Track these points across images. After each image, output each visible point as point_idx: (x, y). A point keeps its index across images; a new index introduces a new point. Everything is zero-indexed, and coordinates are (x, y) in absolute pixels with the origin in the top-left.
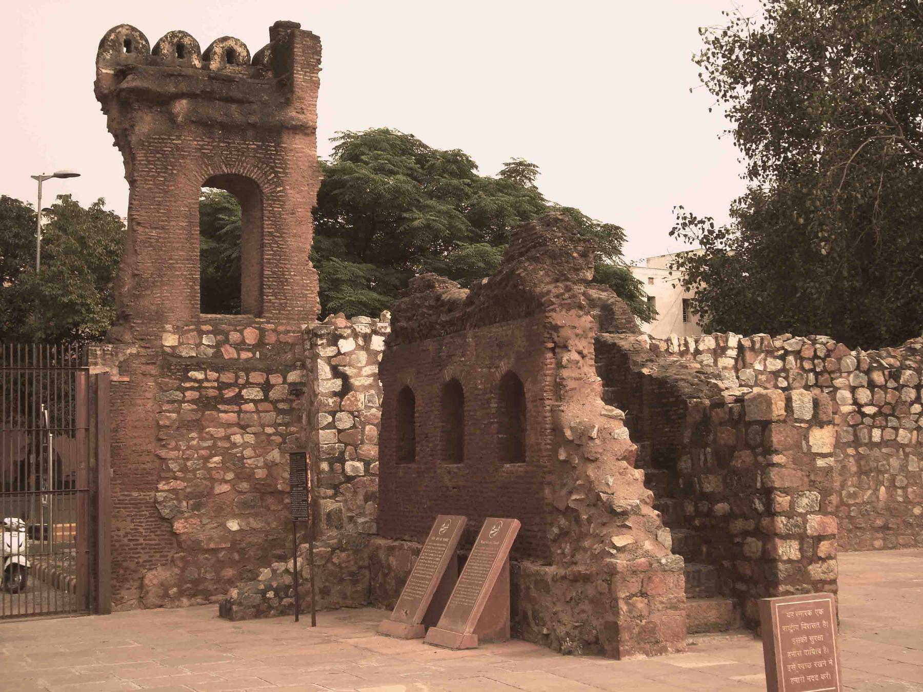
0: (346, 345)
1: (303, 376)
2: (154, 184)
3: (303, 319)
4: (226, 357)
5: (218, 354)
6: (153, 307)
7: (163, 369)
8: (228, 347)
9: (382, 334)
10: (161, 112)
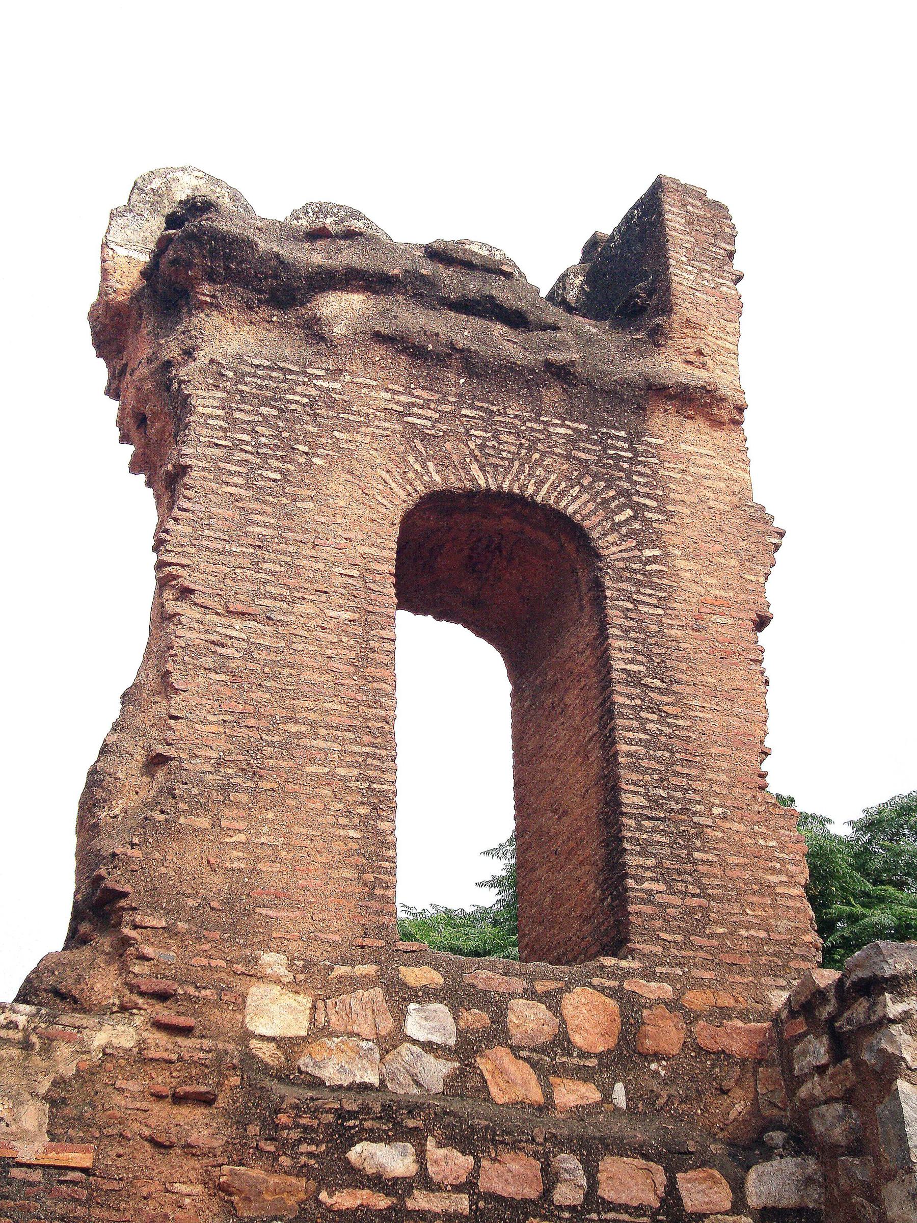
1: (808, 1181)
2: (248, 486)
3: (773, 971)
4: (500, 1098)
5: (466, 1081)
7: (242, 1125)
10: (281, 325)
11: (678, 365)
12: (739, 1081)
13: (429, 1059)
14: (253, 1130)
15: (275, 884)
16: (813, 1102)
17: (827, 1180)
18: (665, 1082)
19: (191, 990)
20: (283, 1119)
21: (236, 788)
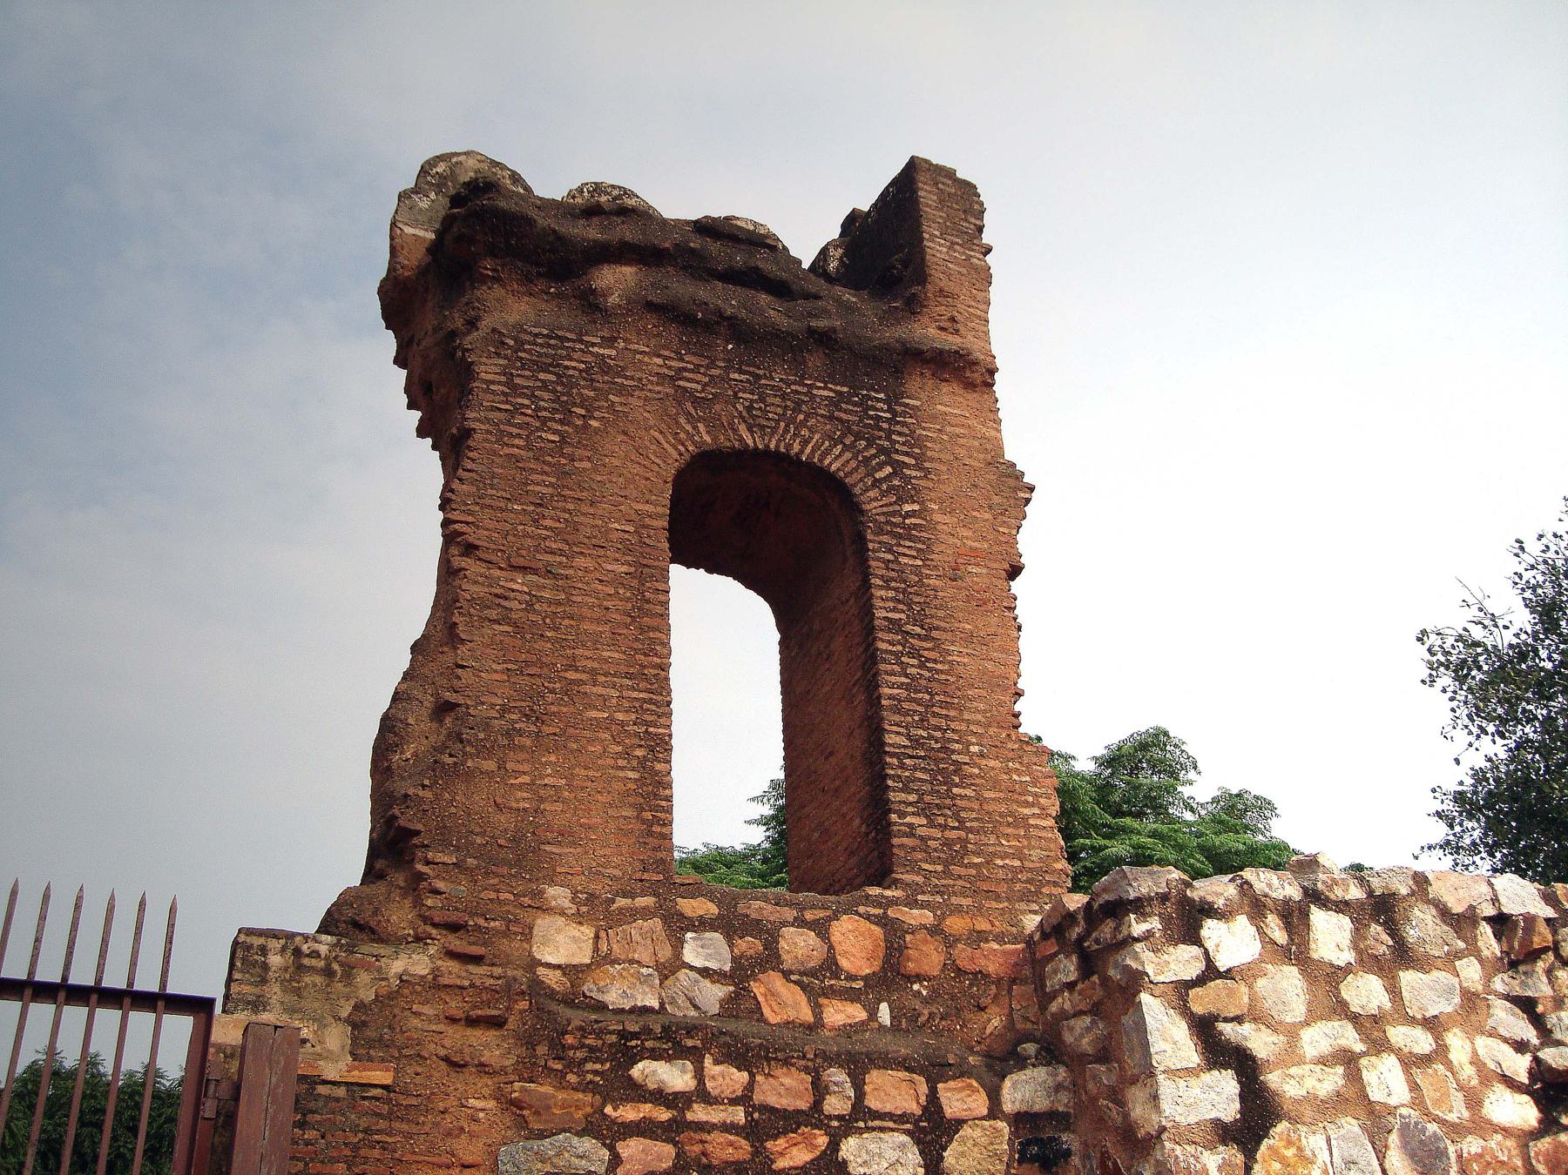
0: (1232, 941)
1: (1058, 1088)
2: (528, 447)
3: (1026, 897)
4: (773, 1019)
5: (740, 1003)
6: (504, 820)
7: (531, 1045)
8: (775, 980)
9: (1342, 907)
10: (558, 296)
11: (932, 331)
12: (995, 998)
13: (706, 983)
14: (541, 1050)
15: (559, 822)
16: (1063, 1016)
17: (1076, 1087)
18: (926, 1001)
19: (481, 922)
20: (569, 1039)
21: (520, 732)
